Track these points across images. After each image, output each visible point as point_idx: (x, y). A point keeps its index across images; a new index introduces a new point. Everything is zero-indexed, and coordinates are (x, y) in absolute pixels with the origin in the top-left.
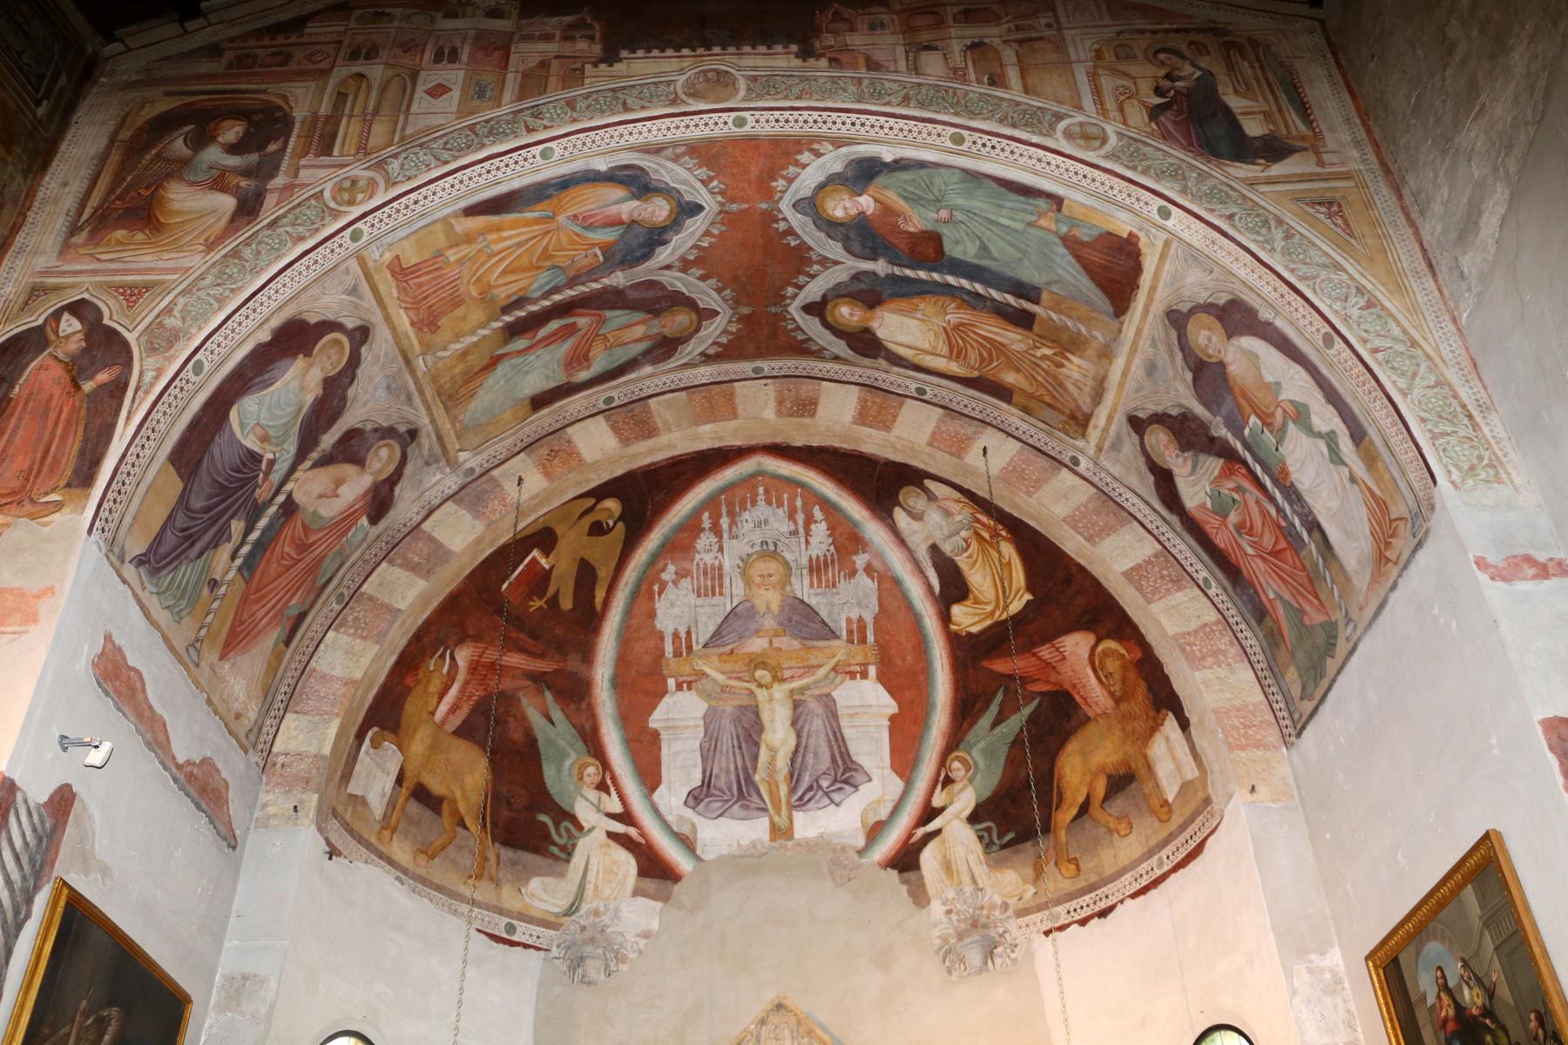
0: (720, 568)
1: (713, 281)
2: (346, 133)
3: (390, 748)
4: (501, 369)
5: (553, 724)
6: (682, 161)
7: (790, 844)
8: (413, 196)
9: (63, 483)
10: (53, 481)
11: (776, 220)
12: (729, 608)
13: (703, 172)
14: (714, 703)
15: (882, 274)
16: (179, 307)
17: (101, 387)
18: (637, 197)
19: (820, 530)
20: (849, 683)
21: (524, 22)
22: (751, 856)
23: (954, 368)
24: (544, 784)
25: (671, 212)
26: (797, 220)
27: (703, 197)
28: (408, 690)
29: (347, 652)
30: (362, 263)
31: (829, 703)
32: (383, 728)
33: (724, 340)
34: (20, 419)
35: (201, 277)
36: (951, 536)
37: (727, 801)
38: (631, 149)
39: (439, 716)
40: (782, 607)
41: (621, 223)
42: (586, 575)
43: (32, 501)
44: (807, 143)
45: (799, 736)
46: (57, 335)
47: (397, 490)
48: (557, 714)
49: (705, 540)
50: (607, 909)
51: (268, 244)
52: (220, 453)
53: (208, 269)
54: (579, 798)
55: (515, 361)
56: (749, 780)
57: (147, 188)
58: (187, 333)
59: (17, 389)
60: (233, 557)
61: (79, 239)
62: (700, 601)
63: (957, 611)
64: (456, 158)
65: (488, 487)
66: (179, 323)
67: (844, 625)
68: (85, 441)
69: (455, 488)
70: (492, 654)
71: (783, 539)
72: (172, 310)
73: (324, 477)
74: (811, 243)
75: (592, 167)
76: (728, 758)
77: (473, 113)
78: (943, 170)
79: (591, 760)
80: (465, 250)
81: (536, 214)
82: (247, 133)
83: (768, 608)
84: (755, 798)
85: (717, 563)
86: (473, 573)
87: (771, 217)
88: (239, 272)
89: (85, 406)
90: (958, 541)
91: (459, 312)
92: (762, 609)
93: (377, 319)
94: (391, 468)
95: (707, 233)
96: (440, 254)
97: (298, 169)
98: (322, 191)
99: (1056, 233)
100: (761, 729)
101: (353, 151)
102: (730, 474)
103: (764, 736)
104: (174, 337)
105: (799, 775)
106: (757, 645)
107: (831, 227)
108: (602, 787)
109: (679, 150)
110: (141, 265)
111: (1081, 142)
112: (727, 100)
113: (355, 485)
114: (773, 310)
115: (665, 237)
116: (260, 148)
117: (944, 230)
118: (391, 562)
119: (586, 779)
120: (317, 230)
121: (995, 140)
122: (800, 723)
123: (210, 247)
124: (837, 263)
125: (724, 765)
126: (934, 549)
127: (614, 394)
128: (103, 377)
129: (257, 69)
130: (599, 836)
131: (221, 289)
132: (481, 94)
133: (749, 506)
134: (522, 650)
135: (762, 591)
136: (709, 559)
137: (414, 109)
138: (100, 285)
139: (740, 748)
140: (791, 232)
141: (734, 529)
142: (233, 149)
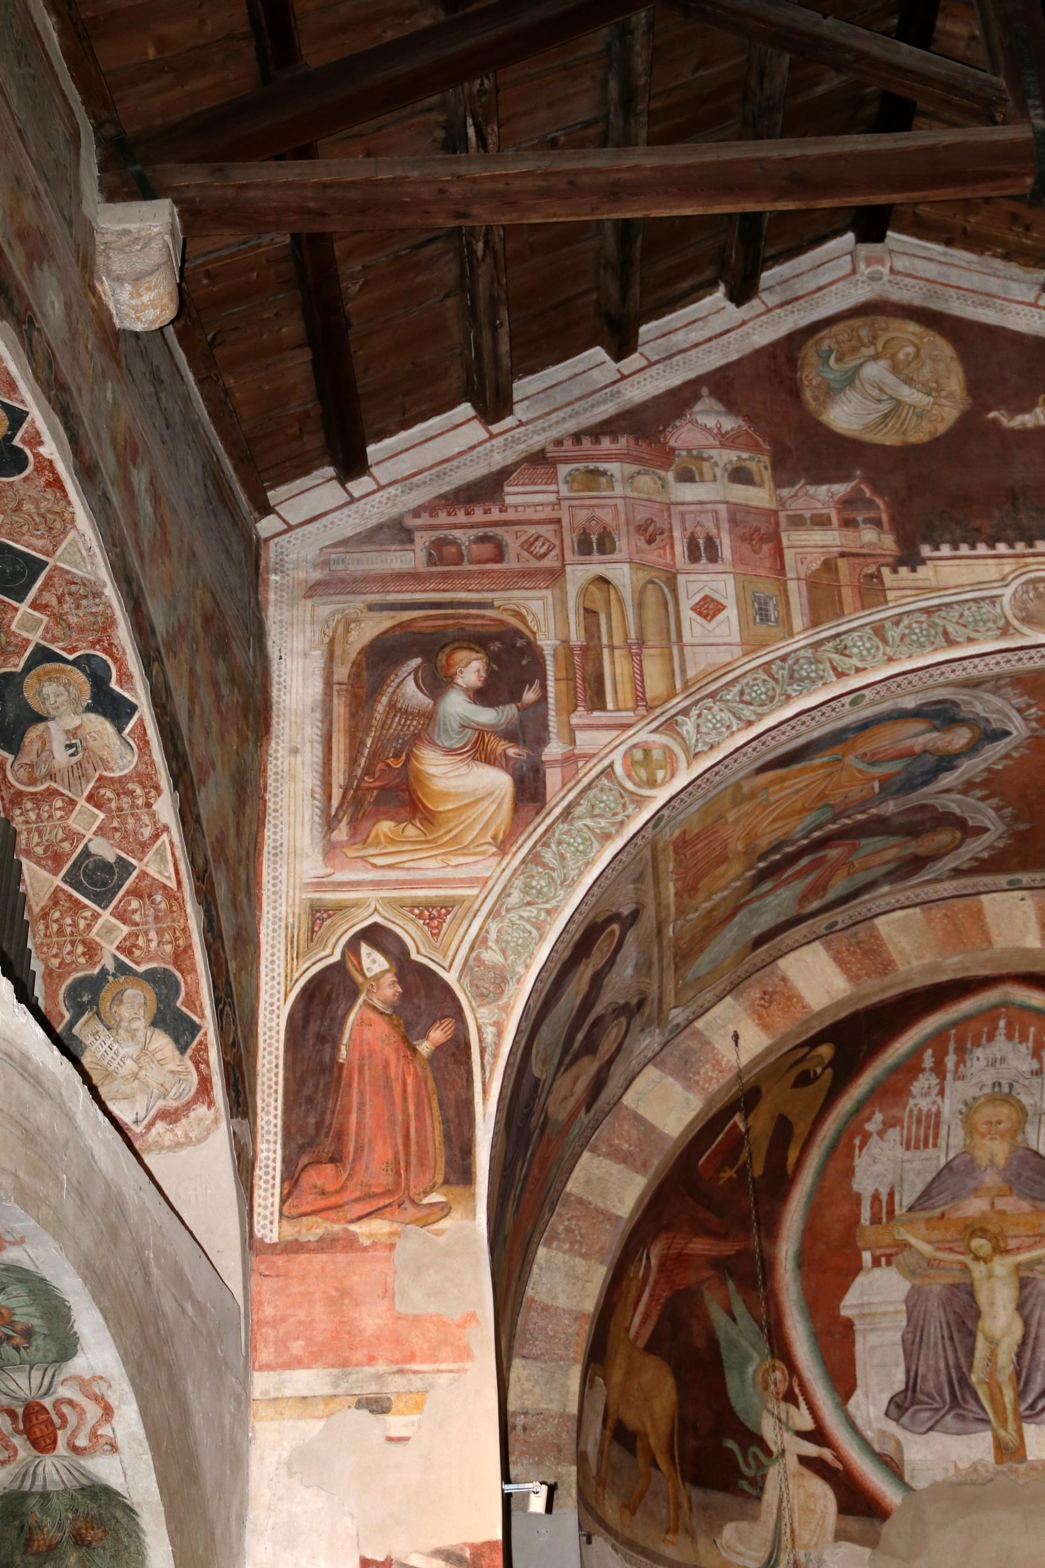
0: (938, 1114)
1: (994, 801)
2: (614, 674)
6: (1002, 691)
7: (1022, 1467)
9: (440, 1179)
10: (428, 1177)
12: (943, 1162)
13: (1021, 701)
14: (918, 1282)
17: (439, 1048)
18: (936, 729)
21: (785, 492)
22: (973, 1483)
24: (727, 1399)
25: (971, 740)
29: (567, 1275)
33: (985, 855)
34: (361, 1093)
35: (505, 893)
37: (937, 1410)
38: (946, 685)
40: (1009, 1161)
43: (413, 1202)
45: (1026, 1324)
46: (364, 975)
48: (739, 1308)
49: (925, 1081)
50: (809, 1561)
51: (569, 844)
53: (510, 880)
54: (765, 1413)
55: (754, 905)
56: (964, 1381)
57: (397, 756)
58: (514, 973)
59: (343, 1052)
61: (341, 833)
62: (908, 1155)
65: (693, 1044)
66: (499, 958)
68: (445, 1121)
70: (679, 1243)
71: (1021, 1080)
72: (485, 940)
75: (899, 706)
76: (936, 1353)
77: (762, 646)
79: (778, 1363)
80: (746, 807)
81: (825, 759)
82: (490, 672)
83: (992, 1161)
84: (973, 1406)
85: (934, 1109)
88: (548, 885)
89: (430, 1074)
92: (985, 1162)
95: (1007, 756)
97: (572, 731)
98: (611, 765)
100: (978, 1315)
101: (630, 704)
103: (980, 1324)
104: (501, 979)
105: (1028, 1375)
106: (975, 1207)
108: (790, 1398)
109: (1002, 682)
110: (430, 875)
115: (955, 763)
116: (515, 696)
120: (622, 823)
122: (1029, 1306)
123: (503, 845)
125: (932, 1362)
128: (438, 1035)
129: (466, 567)
130: (792, 1462)
133: (984, 1041)
135: (986, 1141)
136: (925, 1104)
137: (687, 638)
138: (390, 902)
139: (951, 1339)
141: (962, 1068)
142: (482, 696)
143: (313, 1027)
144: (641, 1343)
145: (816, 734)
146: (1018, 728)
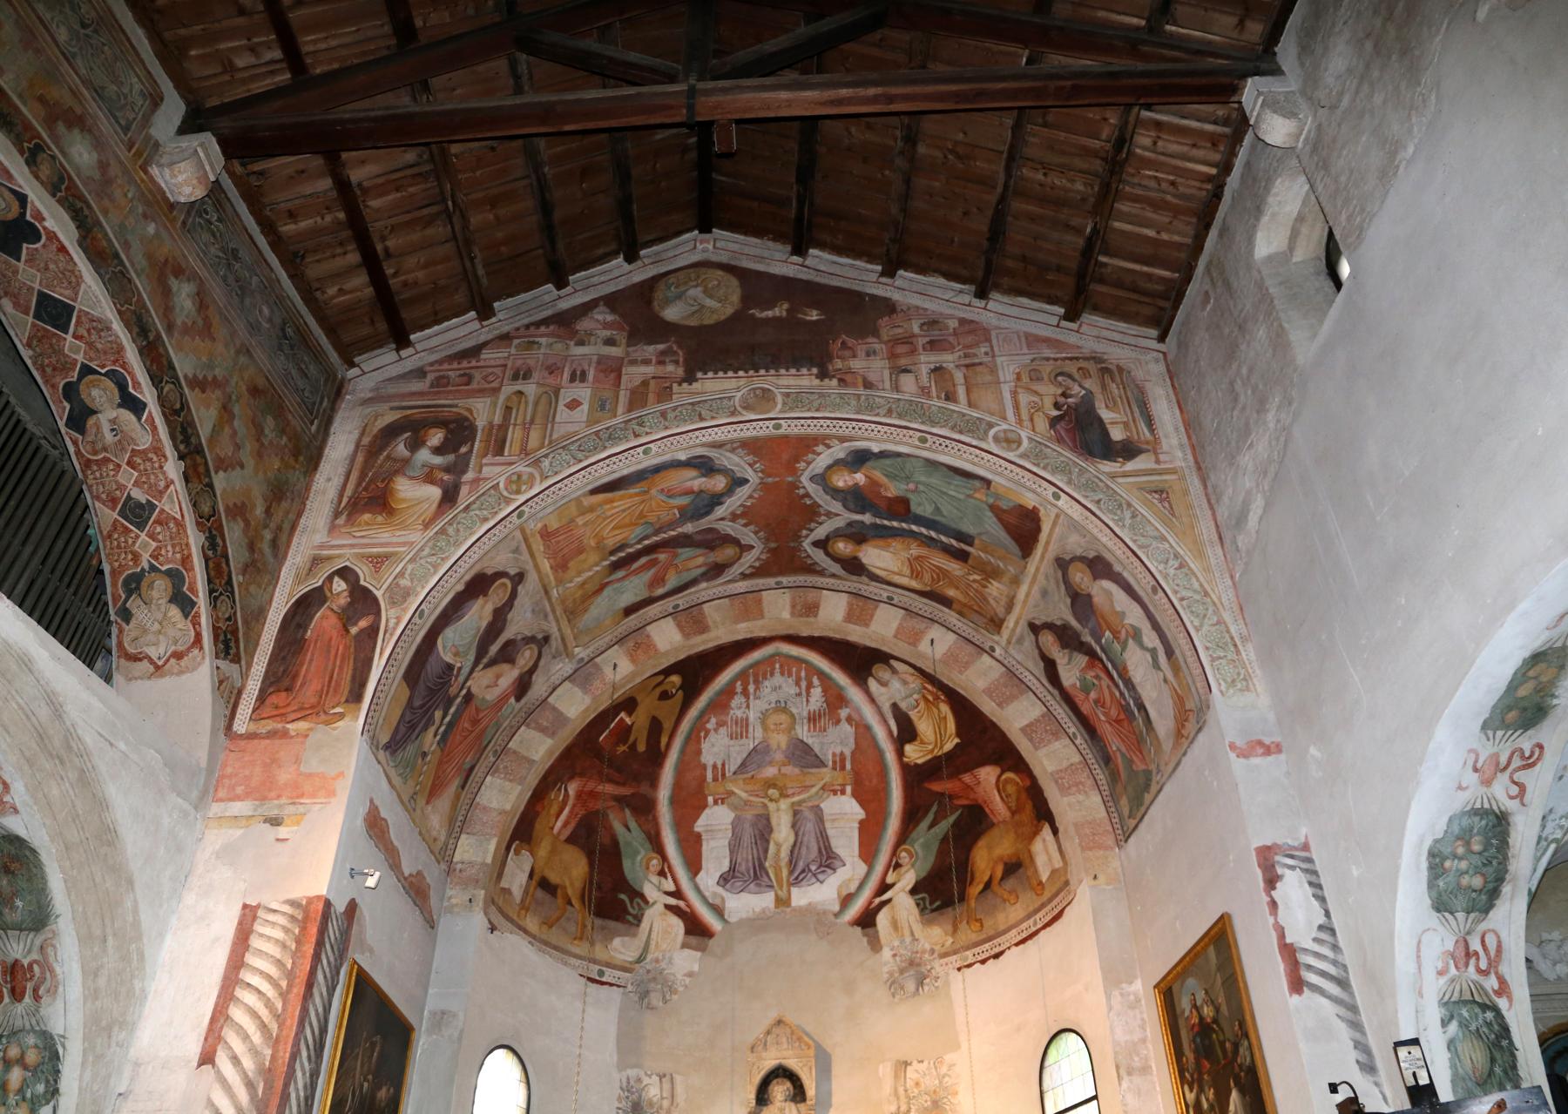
0: (747, 719)
1: (752, 527)
3: (525, 853)
4: (606, 592)
5: (629, 830)
8: (558, 486)
9: (343, 699)
11: (798, 488)
12: (752, 747)
13: (750, 458)
15: (868, 523)
16: (409, 571)
17: (362, 631)
18: (704, 475)
19: (817, 692)
20: (832, 797)
23: (914, 584)
26: (812, 488)
27: (750, 474)
28: (537, 814)
30: (523, 531)
31: (818, 813)
32: (522, 841)
33: (757, 564)
34: (313, 655)
35: (422, 549)
36: (907, 697)
38: (703, 445)
39: (556, 830)
40: (788, 747)
41: (693, 492)
42: (655, 726)
43: (325, 712)
44: (822, 440)
45: (797, 835)
47: (534, 677)
48: (633, 824)
49: (738, 701)
52: (432, 667)
55: (616, 585)
60: (435, 736)
62: (732, 742)
63: (908, 748)
64: (587, 458)
67: (830, 757)
68: (355, 669)
69: (571, 672)
70: (591, 785)
73: (491, 672)
74: (820, 502)
78: (913, 459)
80: (589, 517)
86: (581, 732)
87: (795, 486)
90: (912, 701)
91: (582, 557)
92: (774, 746)
93: (530, 567)
94: (531, 664)
95: (750, 497)
96: (572, 521)
99: (986, 503)
100: (771, 830)
102: (756, 655)
104: (407, 594)
106: (770, 772)
107: (835, 492)
108: (662, 873)
111: (1004, 445)
112: (769, 411)
113: (508, 676)
114: (792, 545)
115: (723, 500)
117: (911, 496)
118: (528, 726)
119: (651, 868)
121: (948, 442)
124: (838, 515)
126: (895, 706)
127: (680, 602)
128: (363, 623)
131: (435, 558)
132: (602, 408)
134: (610, 781)
136: (739, 713)
140: (807, 495)
143: (297, 618)
144: (563, 837)
145: (625, 472)
146: (753, 477)
